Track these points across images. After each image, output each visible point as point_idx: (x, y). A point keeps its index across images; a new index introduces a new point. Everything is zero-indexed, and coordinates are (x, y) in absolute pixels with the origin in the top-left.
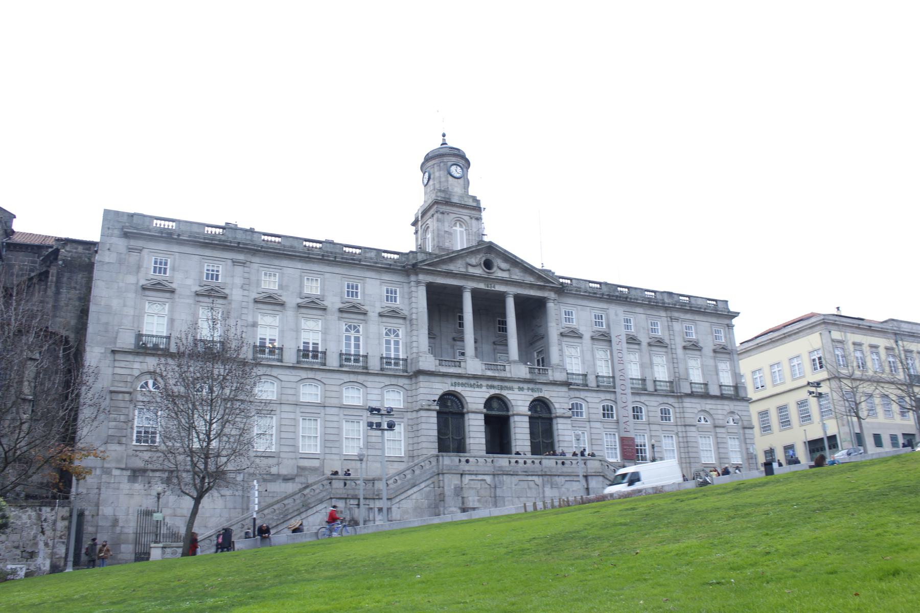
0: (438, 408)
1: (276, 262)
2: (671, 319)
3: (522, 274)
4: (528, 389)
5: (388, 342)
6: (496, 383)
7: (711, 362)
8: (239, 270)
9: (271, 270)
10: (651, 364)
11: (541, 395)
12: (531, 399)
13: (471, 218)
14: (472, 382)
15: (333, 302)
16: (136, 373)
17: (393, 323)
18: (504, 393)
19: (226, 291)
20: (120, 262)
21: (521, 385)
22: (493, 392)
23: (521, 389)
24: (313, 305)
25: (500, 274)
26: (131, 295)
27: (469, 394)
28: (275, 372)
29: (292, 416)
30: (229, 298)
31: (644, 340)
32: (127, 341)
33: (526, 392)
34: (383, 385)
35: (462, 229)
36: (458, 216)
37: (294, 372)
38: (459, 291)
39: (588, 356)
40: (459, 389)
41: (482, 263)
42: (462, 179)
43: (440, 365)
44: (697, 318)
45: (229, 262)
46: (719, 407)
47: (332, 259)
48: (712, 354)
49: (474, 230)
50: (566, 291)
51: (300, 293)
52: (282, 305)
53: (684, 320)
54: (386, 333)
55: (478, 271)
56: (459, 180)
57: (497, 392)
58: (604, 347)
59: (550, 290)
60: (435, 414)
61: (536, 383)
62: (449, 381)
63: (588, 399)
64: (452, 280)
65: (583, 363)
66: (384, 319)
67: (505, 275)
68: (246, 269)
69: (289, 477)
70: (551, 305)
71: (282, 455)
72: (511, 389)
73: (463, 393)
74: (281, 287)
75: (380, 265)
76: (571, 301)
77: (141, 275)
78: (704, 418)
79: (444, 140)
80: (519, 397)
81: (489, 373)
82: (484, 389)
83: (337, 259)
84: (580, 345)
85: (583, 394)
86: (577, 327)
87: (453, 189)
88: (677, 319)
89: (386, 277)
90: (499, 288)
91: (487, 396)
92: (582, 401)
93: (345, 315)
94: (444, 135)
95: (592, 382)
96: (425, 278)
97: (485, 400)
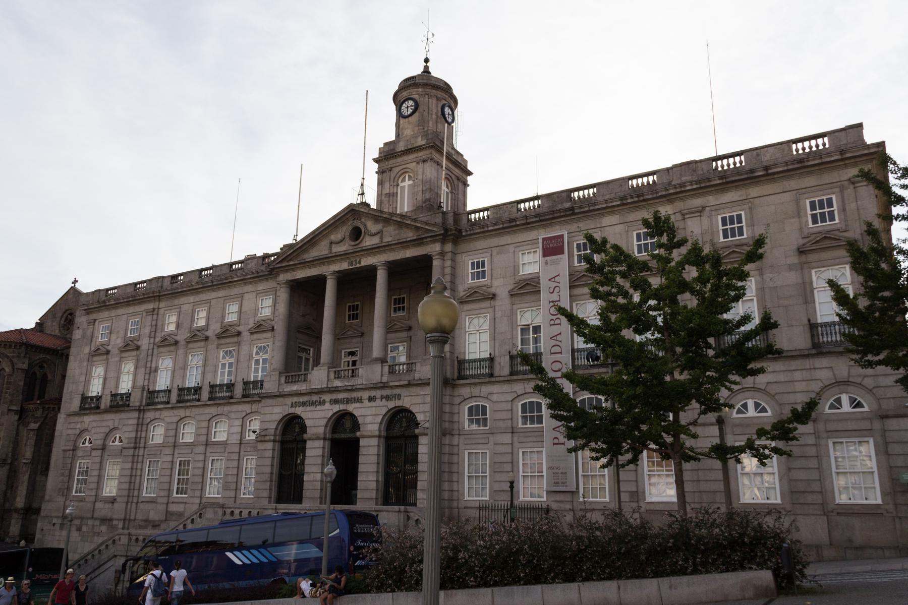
0: (272, 438)
1: (176, 302)
2: (683, 215)
3: (397, 232)
4: (382, 397)
5: (257, 362)
6: (341, 396)
7: (793, 278)
8: (150, 318)
9: (173, 311)
11: (399, 403)
12: (384, 411)
13: (418, 163)
14: (315, 398)
16: (78, 432)
18: (351, 408)
19: (139, 343)
21: (373, 393)
22: (337, 408)
23: (372, 399)
24: (198, 337)
26: (85, 364)
27: (310, 415)
28: (165, 413)
29: (169, 458)
30: (141, 349)
32: (76, 403)
33: (378, 401)
34: (244, 414)
35: (411, 182)
36: (401, 167)
37: (176, 412)
38: (321, 281)
40: (299, 411)
41: (347, 234)
42: (417, 114)
43: (286, 383)
44: (754, 191)
45: (144, 314)
46: (798, 375)
47: (210, 284)
48: (795, 260)
49: (420, 177)
50: (464, 234)
51: (191, 328)
52: (176, 343)
53: (717, 208)
54: (257, 351)
56: (410, 118)
57: (342, 407)
58: (533, 304)
59: (434, 242)
60: (270, 445)
61: (391, 387)
62: (289, 401)
63: (495, 398)
64: (312, 270)
65: (493, 338)
66: (255, 336)
67: (375, 240)
68: (155, 317)
69: (157, 523)
70: (436, 263)
71: (159, 500)
72: (359, 400)
73: (303, 416)
74: (178, 327)
75: (249, 277)
76: (482, 244)
77: (93, 344)
78: (757, 405)
79: (426, 68)
80: (368, 412)
81: (338, 383)
82: (327, 405)
83: (214, 283)
84: (491, 310)
85: (485, 390)
86: (489, 283)
87: (403, 134)
88: (701, 211)
90: (366, 261)
91: (331, 414)
92: (486, 400)
93: (223, 341)
94: (427, 61)
96: (284, 277)
97: (326, 420)
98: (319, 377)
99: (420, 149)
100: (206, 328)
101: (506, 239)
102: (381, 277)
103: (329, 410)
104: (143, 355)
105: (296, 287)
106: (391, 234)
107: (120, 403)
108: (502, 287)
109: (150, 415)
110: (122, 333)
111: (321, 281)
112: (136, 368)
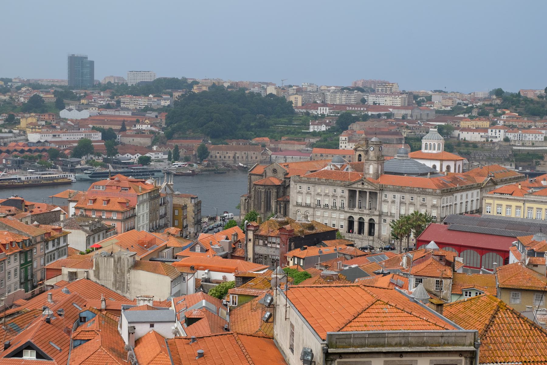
10: (409, 209)
15: (331, 194)
17: (342, 199)
20: (294, 187)
22: (360, 216)
25: (366, 187)
31: (407, 202)
32: (295, 204)
38: (355, 191)
39: (389, 207)
40: (352, 216)
55: (360, 186)
70: (378, 194)
76: (387, 192)
81: (360, 212)
89: (341, 188)
95: (389, 214)
98: (356, 210)
99: (374, 160)
100: (328, 193)
101: (390, 192)
102: (368, 194)
103: (358, 217)
104: (312, 196)
105: (350, 191)
106: (370, 187)
107: (308, 206)
108: (390, 201)
109: (316, 209)
110: (305, 189)
111: (355, 191)
112: (311, 198)
